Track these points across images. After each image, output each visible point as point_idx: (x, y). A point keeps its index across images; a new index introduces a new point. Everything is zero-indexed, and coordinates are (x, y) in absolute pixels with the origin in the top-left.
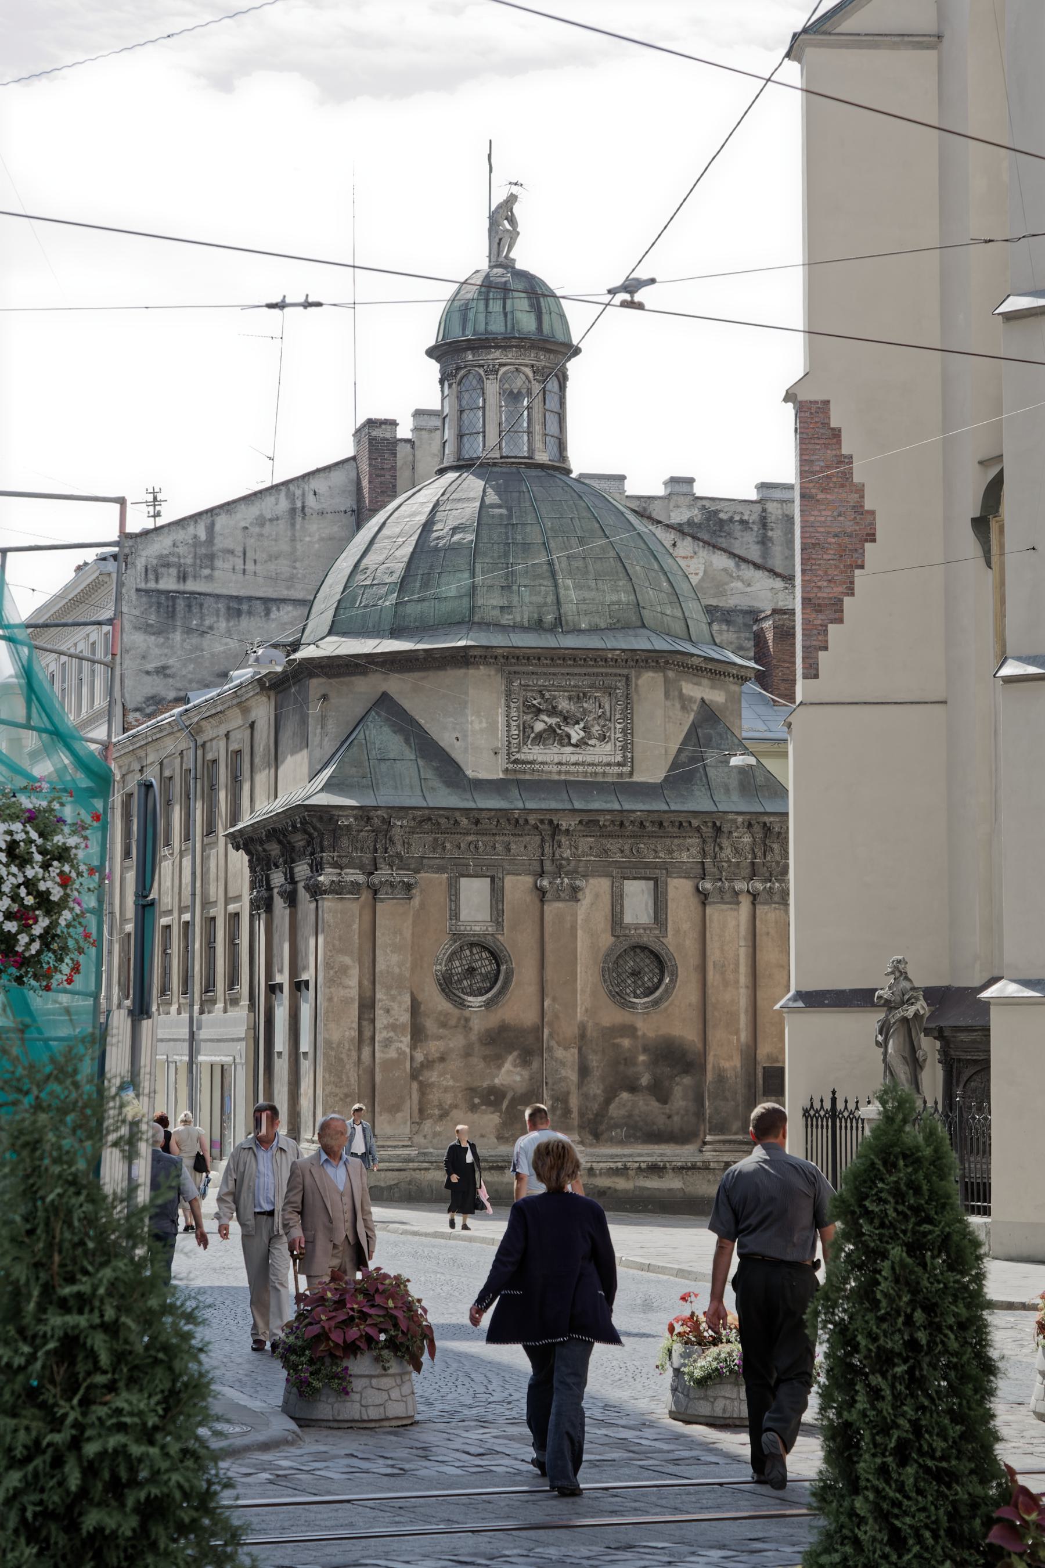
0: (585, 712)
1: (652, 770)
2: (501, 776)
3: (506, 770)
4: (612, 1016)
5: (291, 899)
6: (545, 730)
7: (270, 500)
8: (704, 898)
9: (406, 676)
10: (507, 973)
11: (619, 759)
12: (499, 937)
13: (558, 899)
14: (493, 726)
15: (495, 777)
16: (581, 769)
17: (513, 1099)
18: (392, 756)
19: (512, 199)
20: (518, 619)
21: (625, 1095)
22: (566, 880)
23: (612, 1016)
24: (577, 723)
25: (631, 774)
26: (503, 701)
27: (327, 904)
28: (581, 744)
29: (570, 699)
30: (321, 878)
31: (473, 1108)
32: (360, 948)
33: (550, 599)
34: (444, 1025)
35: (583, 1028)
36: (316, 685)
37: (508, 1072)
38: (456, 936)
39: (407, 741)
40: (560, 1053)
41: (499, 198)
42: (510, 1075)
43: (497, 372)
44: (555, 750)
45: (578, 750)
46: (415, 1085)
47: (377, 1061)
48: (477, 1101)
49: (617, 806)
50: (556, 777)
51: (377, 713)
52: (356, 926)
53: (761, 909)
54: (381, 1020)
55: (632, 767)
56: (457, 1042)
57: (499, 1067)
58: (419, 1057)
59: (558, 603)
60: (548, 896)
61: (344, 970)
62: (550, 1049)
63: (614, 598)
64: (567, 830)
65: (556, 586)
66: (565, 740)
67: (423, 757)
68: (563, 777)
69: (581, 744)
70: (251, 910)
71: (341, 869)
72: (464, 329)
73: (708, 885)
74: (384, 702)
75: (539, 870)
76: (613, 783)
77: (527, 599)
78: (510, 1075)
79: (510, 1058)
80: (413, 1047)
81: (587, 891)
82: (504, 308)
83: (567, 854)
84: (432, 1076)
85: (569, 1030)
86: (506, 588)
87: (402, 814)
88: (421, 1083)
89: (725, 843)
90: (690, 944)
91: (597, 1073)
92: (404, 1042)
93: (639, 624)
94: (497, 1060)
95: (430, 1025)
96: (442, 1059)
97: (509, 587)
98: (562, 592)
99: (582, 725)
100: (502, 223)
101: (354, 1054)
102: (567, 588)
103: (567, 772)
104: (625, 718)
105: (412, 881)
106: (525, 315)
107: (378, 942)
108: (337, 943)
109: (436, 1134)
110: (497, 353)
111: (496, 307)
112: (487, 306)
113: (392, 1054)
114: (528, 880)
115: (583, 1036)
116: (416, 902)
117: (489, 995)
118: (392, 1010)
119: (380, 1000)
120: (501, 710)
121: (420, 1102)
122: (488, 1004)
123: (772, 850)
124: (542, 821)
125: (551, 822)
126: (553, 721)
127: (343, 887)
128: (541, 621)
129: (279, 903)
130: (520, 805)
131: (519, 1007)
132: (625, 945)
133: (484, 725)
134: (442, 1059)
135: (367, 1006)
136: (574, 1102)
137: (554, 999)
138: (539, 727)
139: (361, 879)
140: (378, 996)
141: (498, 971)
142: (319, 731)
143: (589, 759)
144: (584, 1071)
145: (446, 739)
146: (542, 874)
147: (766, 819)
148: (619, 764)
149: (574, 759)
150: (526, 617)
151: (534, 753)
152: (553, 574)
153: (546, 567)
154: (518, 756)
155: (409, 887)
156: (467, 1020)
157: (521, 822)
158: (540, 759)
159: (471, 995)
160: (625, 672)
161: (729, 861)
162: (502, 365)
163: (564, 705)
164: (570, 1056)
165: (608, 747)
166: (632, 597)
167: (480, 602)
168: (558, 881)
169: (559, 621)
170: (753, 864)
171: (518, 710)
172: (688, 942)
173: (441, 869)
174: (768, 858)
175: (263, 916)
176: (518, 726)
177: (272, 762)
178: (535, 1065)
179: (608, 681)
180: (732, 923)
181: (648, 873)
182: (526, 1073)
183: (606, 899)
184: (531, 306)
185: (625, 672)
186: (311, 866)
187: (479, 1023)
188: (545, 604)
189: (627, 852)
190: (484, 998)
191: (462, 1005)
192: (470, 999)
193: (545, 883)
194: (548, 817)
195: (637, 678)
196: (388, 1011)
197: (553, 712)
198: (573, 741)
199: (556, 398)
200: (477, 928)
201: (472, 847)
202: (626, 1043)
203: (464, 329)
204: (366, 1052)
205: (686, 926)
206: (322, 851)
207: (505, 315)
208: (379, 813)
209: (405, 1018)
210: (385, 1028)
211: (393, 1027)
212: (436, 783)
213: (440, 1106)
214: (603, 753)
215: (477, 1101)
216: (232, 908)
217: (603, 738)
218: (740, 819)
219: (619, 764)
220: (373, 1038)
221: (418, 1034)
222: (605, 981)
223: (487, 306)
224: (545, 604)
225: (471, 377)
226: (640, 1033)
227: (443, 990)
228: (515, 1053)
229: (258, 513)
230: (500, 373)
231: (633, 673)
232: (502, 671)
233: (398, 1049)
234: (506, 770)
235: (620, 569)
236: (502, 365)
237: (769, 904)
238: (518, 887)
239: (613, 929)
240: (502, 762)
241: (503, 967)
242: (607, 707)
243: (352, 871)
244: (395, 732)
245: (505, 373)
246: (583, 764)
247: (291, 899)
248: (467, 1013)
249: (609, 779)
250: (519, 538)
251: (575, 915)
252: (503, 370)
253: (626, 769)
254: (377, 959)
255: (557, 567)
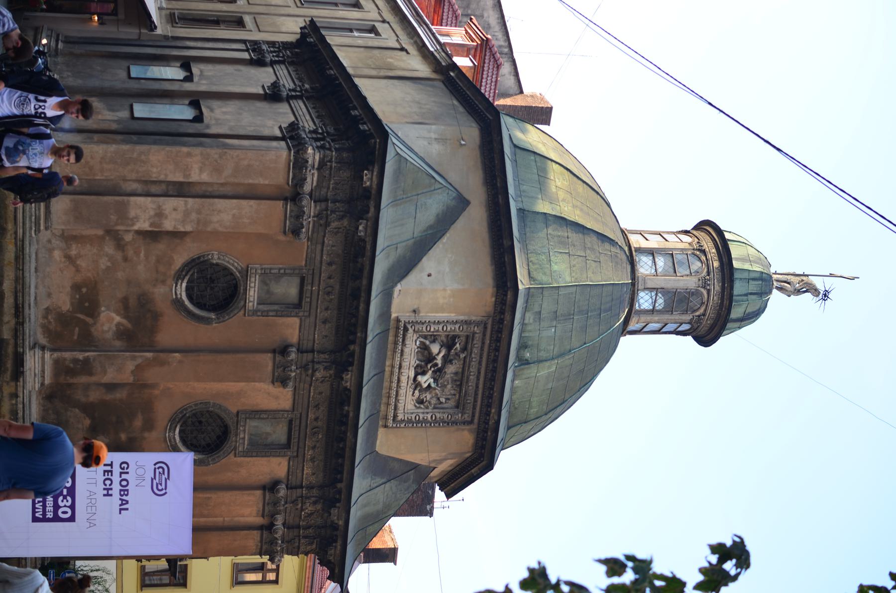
0: (444, 386)
1: (388, 444)
2: (394, 315)
3: (398, 320)
4: (164, 410)
5: (273, 95)
6: (430, 353)
7: (500, 35)
8: (271, 487)
9: (485, 224)
10: (208, 319)
11: (400, 417)
12: (242, 312)
13: (275, 366)
14: (442, 309)
15: (394, 308)
16: (394, 385)
17: (86, 323)
18: (418, 215)
19: (814, 291)
20: (529, 328)
21: (87, 422)
22: (293, 374)
23: (164, 410)
24: (436, 380)
25: (386, 426)
26: (462, 318)
27: (285, 153)
28: (417, 385)
29: (456, 373)
30: (310, 151)
31: (76, 287)
32: (238, 184)
33: (543, 355)
34: (158, 261)
35: (153, 386)
36: (472, 132)
37: (113, 319)
38: (245, 273)
39: (430, 227)
40: (130, 366)
41: (819, 283)
42: (109, 320)
43: (704, 288)
44: (413, 363)
45: (411, 381)
46: (100, 232)
47: (125, 198)
48: (84, 290)
49: (361, 422)
50: (388, 363)
51: (454, 198)
52: (262, 181)
53: (256, 534)
54: (169, 204)
55: (392, 427)
56: (142, 271)
57: (118, 313)
58: (128, 237)
59: (540, 361)
60: (279, 358)
61: (218, 170)
62: (134, 358)
63: (534, 404)
64: (342, 379)
65: (553, 359)
66: (420, 371)
67: (415, 243)
68: (387, 369)
69: (417, 385)
70: (250, 41)
71: (318, 169)
72: (737, 259)
73: (282, 492)
74: (462, 203)
75: (304, 348)
76: (379, 412)
77: (545, 334)
78: (109, 320)
79: (124, 321)
80: (140, 233)
81: (281, 389)
82: (751, 294)
83: (318, 375)
84: (109, 248)
85: (152, 375)
86: (555, 316)
87: (369, 231)
88: (102, 238)
89: (319, 507)
90: (228, 477)
91: (109, 397)
92: (144, 225)
93: (510, 424)
94: (125, 307)
95: (160, 247)
96: (126, 259)
97: (556, 318)
98: (547, 364)
99: (433, 385)
100: (801, 286)
101: (134, 176)
102: (549, 367)
103: (392, 373)
104: (435, 421)
105: (303, 236)
106: (743, 310)
107: (244, 202)
108: (245, 163)
109: (50, 251)
110: (718, 288)
111: (753, 287)
112: (754, 279)
113: (132, 214)
114: (295, 339)
115: (145, 386)
116: (282, 238)
117: (187, 302)
118: (175, 213)
119: (186, 203)
120: (453, 316)
121: (82, 237)
122: (177, 303)
123: (312, 543)
124: (352, 354)
125: (352, 364)
126: (439, 361)
127: (301, 169)
128: (526, 347)
129: (264, 77)
130: (369, 339)
131: (175, 330)
132: (230, 422)
133: (441, 301)
134: (126, 259)
135: (181, 190)
136: (83, 379)
137: (180, 362)
138: (435, 348)
139: (307, 188)
140: (190, 200)
141: (209, 310)
142: (433, 136)
143: (402, 392)
144: (111, 387)
145: (429, 263)
146: (300, 351)
147: (339, 543)
148: (395, 416)
149: (404, 379)
150: (531, 334)
151: (412, 345)
152: (561, 355)
153: (568, 347)
154: (411, 331)
155: (296, 232)
156: (163, 282)
157: (351, 337)
158: (407, 350)
159: (187, 289)
160: (476, 421)
161: (302, 510)
162: (709, 291)
163: (451, 369)
164: (127, 376)
165: (410, 406)
166: (532, 417)
167: (546, 293)
168: (293, 368)
169: (527, 363)
170: (298, 527)
171: (451, 330)
172: (229, 474)
173: (309, 259)
174: (302, 541)
175: (246, 55)
176: (438, 331)
177: (383, 73)
178: (118, 344)
179: (469, 407)
180: (247, 511)
181: (294, 441)
182: (109, 335)
183: (273, 405)
184: (749, 314)
185: (476, 421)
186: (315, 132)
187: (159, 292)
188: (539, 350)
189: (315, 423)
190: (184, 297)
191: (179, 277)
192: (184, 285)
193: (293, 356)
194: (356, 362)
195: (470, 431)
196: (175, 210)
197: (447, 360)
198: (419, 378)
199: (672, 330)
200: (252, 293)
201: (329, 289)
202: (138, 422)
203: (737, 259)
204: (135, 186)
205: (243, 472)
206: (335, 149)
207: (746, 295)
208: (372, 209)
209: (168, 225)
210: (159, 207)
211: (160, 214)
212: (393, 258)
213: (79, 256)
214: (407, 402)
215: (84, 290)
216: (247, 19)
217: (420, 402)
218: (341, 523)
219: (395, 416)
220: (148, 194)
221: (153, 236)
222: (196, 405)
223: (754, 279)
224: (539, 350)
225: (699, 264)
226: (146, 435)
227: (193, 260)
228: (129, 326)
229: (492, 26)
230: (702, 290)
231: (474, 426)
232: (489, 317)
233: (137, 218)
234: (398, 320)
235: (555, 405)
236: (709, 291)
237: (261, 541)
238: (290, 328)
239: (245, 412)
240: (406, 317)
241: (213, 316)
242: (445, 405)
243: (315, 179)
244: (438, 215)
245: (702, 294)
246: (398, 386)
247: (273, 95)
248: (170, 281)
249: (383, 408)
250: (590, 321)
251: (260, 380)
252: (705, 292)
253: (390, 423)
254: (227, 201)
255: (567, 357)
